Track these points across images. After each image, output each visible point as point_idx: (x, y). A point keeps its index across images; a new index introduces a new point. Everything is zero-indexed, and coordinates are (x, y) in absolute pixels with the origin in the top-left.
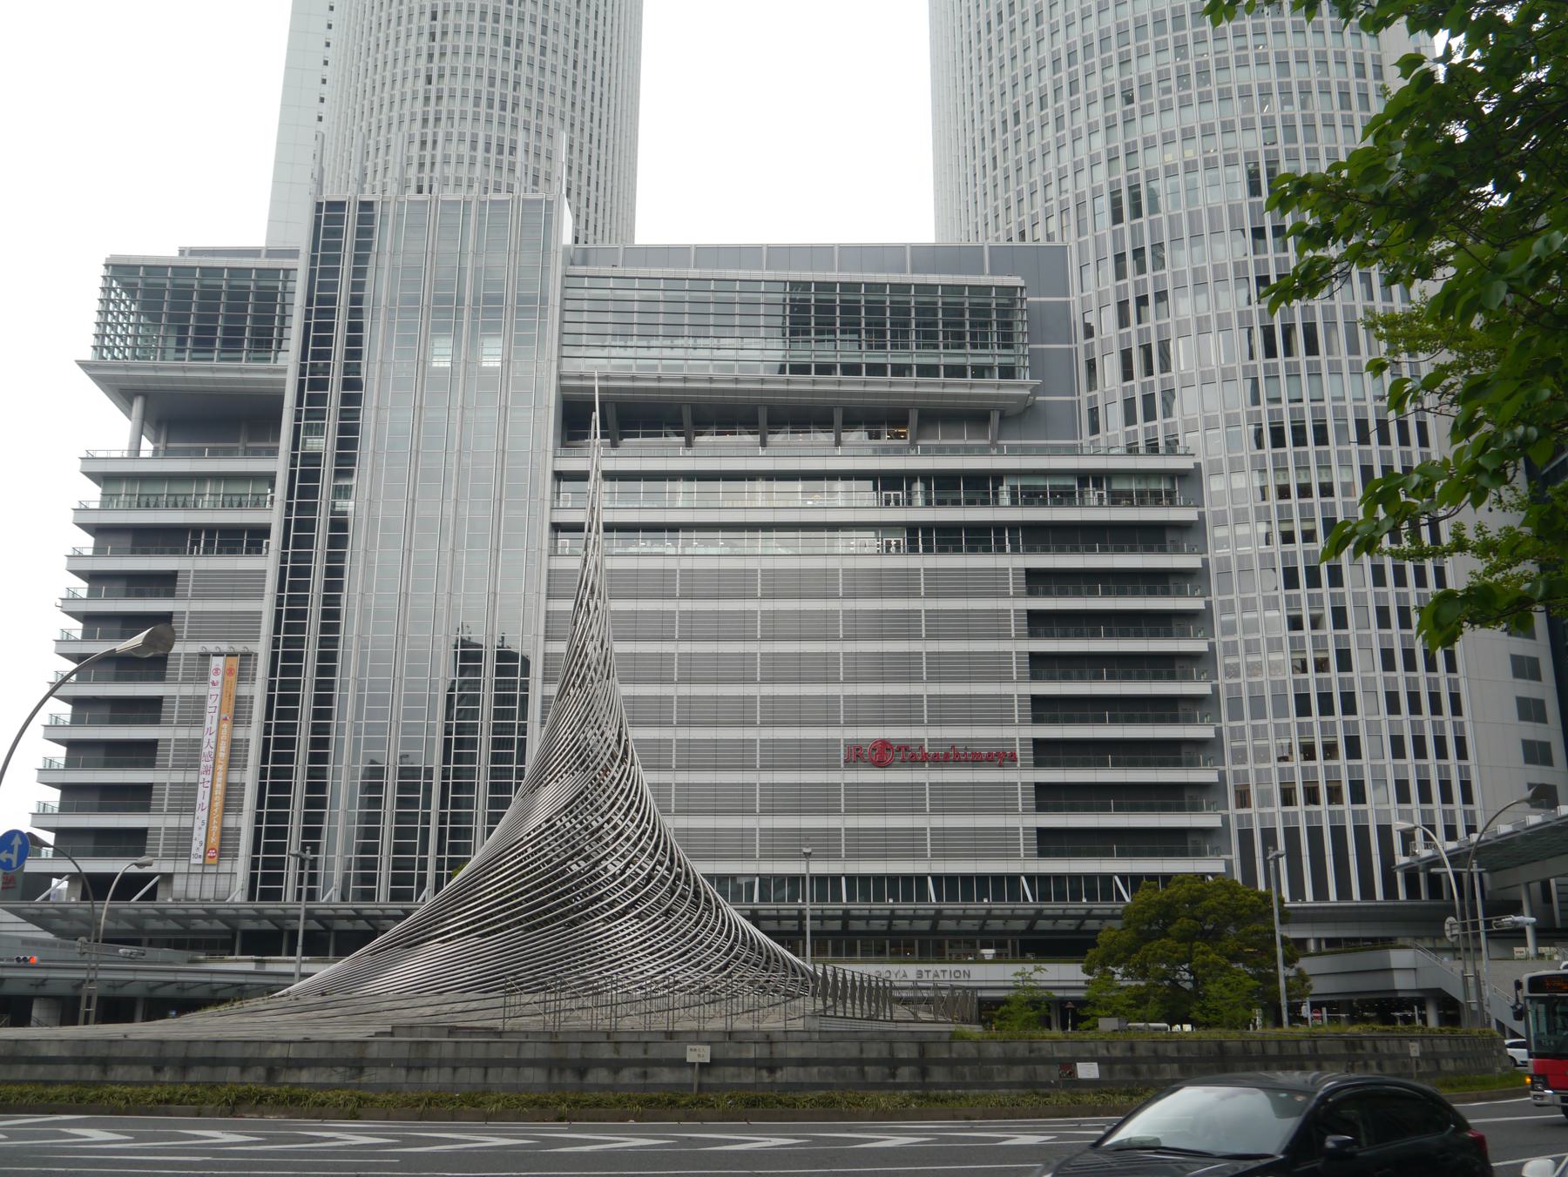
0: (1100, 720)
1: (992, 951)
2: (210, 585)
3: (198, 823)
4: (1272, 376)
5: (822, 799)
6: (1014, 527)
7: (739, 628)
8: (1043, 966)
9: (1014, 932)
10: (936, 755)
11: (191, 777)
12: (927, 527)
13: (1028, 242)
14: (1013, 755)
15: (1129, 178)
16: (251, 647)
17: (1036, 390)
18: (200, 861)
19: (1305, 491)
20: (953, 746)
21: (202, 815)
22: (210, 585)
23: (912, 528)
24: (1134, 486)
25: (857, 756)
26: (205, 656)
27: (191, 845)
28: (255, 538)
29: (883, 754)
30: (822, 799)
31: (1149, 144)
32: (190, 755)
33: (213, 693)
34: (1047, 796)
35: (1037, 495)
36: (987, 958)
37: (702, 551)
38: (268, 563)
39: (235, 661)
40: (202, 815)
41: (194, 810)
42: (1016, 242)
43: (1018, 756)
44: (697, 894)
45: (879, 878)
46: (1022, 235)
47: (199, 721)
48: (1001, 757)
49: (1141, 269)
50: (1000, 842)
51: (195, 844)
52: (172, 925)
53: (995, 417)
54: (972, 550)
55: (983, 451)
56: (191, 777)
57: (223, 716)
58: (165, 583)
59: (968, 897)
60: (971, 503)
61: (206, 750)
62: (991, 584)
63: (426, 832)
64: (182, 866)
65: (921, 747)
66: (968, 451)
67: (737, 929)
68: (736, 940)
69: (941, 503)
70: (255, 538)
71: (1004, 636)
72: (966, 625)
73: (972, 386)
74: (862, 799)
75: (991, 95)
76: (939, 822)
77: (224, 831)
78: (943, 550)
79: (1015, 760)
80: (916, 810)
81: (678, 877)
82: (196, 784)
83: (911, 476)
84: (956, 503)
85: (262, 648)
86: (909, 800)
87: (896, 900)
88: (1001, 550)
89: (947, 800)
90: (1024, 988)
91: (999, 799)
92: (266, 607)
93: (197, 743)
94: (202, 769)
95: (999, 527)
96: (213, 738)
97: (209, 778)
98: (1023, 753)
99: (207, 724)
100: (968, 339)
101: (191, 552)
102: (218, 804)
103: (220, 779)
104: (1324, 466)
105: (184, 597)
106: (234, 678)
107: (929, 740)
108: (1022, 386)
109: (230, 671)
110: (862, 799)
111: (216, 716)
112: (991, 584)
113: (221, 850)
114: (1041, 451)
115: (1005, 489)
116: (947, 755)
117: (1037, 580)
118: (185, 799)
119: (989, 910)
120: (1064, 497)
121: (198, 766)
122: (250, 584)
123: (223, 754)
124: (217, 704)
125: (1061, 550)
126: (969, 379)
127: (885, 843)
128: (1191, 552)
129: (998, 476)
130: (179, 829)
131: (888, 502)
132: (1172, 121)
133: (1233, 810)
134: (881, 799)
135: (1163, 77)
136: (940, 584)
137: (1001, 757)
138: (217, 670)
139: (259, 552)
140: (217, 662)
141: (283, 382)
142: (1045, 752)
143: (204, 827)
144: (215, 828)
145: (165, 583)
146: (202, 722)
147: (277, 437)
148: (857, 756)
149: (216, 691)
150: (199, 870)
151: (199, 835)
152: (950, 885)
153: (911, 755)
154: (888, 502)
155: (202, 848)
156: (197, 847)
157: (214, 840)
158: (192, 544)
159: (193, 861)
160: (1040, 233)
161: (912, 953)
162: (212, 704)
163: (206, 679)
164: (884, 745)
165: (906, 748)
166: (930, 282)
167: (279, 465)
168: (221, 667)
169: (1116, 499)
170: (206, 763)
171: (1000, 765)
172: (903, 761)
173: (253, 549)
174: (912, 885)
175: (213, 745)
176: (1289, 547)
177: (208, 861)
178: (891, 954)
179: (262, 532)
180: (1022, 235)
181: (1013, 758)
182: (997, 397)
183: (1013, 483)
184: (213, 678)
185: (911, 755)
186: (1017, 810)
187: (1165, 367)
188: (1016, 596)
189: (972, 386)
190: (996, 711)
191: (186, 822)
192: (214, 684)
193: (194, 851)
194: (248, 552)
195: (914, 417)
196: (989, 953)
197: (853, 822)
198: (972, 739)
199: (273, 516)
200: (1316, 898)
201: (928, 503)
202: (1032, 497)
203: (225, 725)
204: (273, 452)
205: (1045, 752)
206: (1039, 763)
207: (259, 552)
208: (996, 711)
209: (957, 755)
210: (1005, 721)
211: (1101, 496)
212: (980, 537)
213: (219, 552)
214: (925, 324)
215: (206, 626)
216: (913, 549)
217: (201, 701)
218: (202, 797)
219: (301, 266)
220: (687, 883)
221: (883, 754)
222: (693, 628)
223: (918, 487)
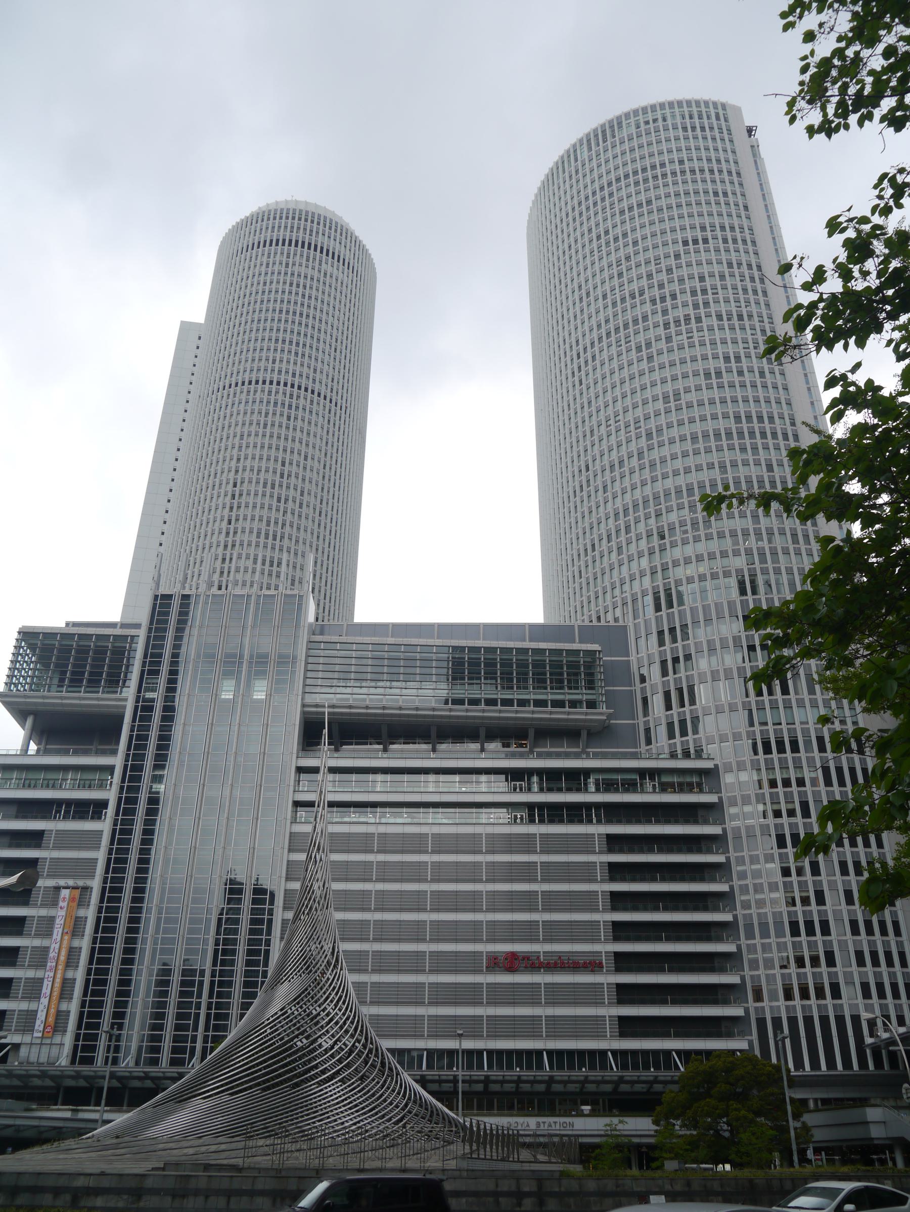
0: (658, 939)
1: (589, 1107)
2: (66, 840)
3: (41, 1007)
4: (761, 708)
5: (470, 994)
6: (598, 806)
7: (415, 873)
9: (604, 1093)
10: (549, 963)
11: (39, 974)
12: (541, 806)
13: (603, 623)
14: (601, 963)
15: (664, 584)
16: (89, 883)
17: (610, 716)
18: (40, 1035)
19: (787, 783)
20: (560, 957)
21: (44, 1001)
22: (66, 840)
23: (531, 806)
24: (675, 779)
25: (496, 963)
26: (58, 889)
27: (35, 1023)
28: (97, 809)
29: (512, 963)
30: (470, 994)
31: (676, 564)
32: (40, 957)
33: (60, 914)
34: (625, 994)
35: (613, 785)
36: (585, 1112)
37: (392, 820)
38: (105, 826)
39: (77, 893)
40: (44, 1001)
41: (39, 998)
42: (595, 623)
44: (383, 1064)
45: (509, 1052)
46: (599, 618)
47: (49, 934)
48: (592, 965)
49: (674, 640)
50: (592, 1027)
51: (38, 1022)
52: (16, 1082)
53: (584, 734)
54: (571, 821)
55: (577, 756)
56: (39, 974)
57: (66, 931)
58: (35, 838)
59: (571, 1067)
60: (569, 790)
61: (52, 954)
62: (583, 844)
63: (197, 1016)
64: (27, 1039)
65: (538, 957)
66: (567, 756)
67: (410, 1090)
68: (409, 1099)
69: (550, 790)
70: (97, 809)
71: (592, 880)
73: (569, 713)
74: (498, 995)
75: (577, 534)
76: (551, 1011)
77: (59, 1013)
78: (551, 821)
79: (602, 967)
80: (536, 1003)
81: (370, 1051)
82: (43, 979)
83: (530, 772)
84: (560, 790)
85: (96, 884)
86: (529, 994)
87: (522, 1068)
88: (590, 821)
89: (556, 995)
90: (611, 1136)
91: (590, 995)
92: (101, 855)
93: (46, 950)
94: (48, 968)
95: (588, 806)
96: (57, 946)
97: (52, 974)
99: (55, 936)
100: (566, 683)
101: (55, 817)
102: (56, 994)
103: (59, 976)
104: (798, 767)
105: (47, 848)
106: (75, 904)
107: (544, 952)
108: (601, 714)
109: (72, 899)
110: (498, 995)
111: (60, 930)
112: (583, 844)
113: (55, 1027)
114: (614, 756)
115: (591, 780)
116: (556, 963)
117: (614, 843)
118: (34, 989)
119: (587, 1077)
120: (630, 786)
121: (46, 966)
122: (91, 840)
123: (63, 958)
124: (62, 922)
125: (629, 822)
126: (567, 709)
127: (515, 1026)
128: (715, 823)
129: (587, 772)
130: (28, 1011)
131: (515, 789)
132: (689, 550)
133: (751, 1004)
134: (513, 995)
135: (682, 524)
136: (550, 844)
137: (592, 965)
138: (64, 898)
139: (100, 818)
140: (65, 893)
141: (125, 707)
142: (623, 962)
143: (45, 1011)
144: (53, 1011)
145: (35, 838)
146: (51, 935)
147: (118, 742)
148: (496, 963)
149: (62, 913)
150: (39, 1041)
151: (41, 1016)
152: (558, 1056)
153: (531, 963)
154: (515, 789)
155: (42, 1026)
156: (39, 1025)
157: (51, 1019)
158: (56, 813)
159: (36, 1035)
160: (610, 617)
161: (533, 1108)
162: (59, 922)
163: (57, 905)
164: (513, 955)
165: (528, 958)
166: (541, 647)
167: (117, 761)
168: (67, 897)
170: (51, 964)
171: (592, 971)
172: (526, 967)
173: (96, 816)
174: (531, 1058)
175: (57, 951)
176: (779, 821)
177: (46, 1035)
178: (518, 1109)
179: (104, 804)
180: (599, 618)
181: (600, 965)
182: (585, 720)
183: (597, 777)
184: (61, 904)
185: (531, 963)
186: (604, 1003)
187: (693, 702)
188: (601, 852)
189: (569, 713)
190: (588, 932)
191: (33, 1006)
192: (61, 908)
193: (36, 1027)
194: (92, 818)
195: (531, 733)
196: (587, 1108)
197: (492, 1011)
198: (573, 952)
199: (111, 795)
200: (812, 1068)
201: (541, 790)
202: (609, 786)
203: (66, 937)
204: (114, 752)
205: (623, 962)
206: (619, 969)
207: (100, 818)
208: (588, 932)
209: (563, 963)
210: (595, 940)
211: (654, 786)
212: (575, 813)
213: (74, 818)
214: (539, 674)
215: (60, 868)
216: (532, 821)
217: (52, 920)
218: (46, 989)
219: (142, 633)
220: (376, 1056)
221: (512, 963)
222: (386, 873)
223: (535, 779)
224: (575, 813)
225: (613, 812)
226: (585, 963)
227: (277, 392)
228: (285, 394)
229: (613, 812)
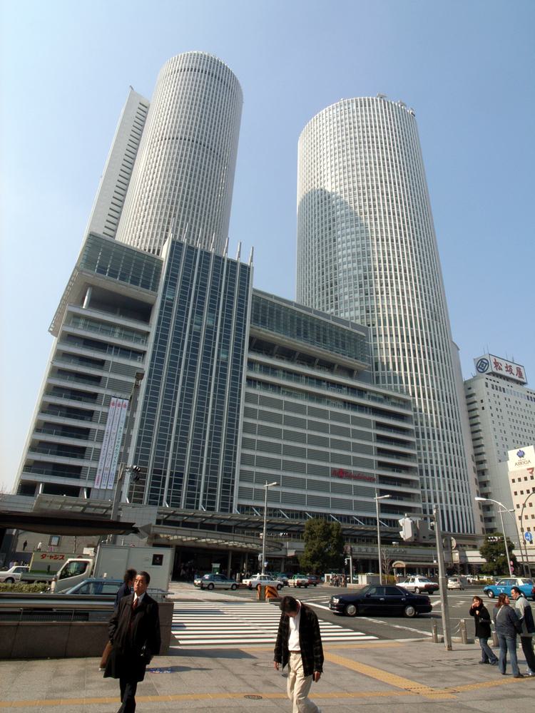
22: (118, 368)
28: (140, 354)
29: (340, 474)
62: (365, 423)
86: (346, 489)
112: (365, 423)
117: (379, 425)
120: (380, 401)
141: (155, 302)
145: (100, 364)
169: (394, 404)
179: (143, 353)
199: (149, 348)
202: (374, 399)
212: (362, 408)
221: (340, 474)
222: (289, 421)
224: (362, 408)
225: (376, 411)
229: (376, 411)
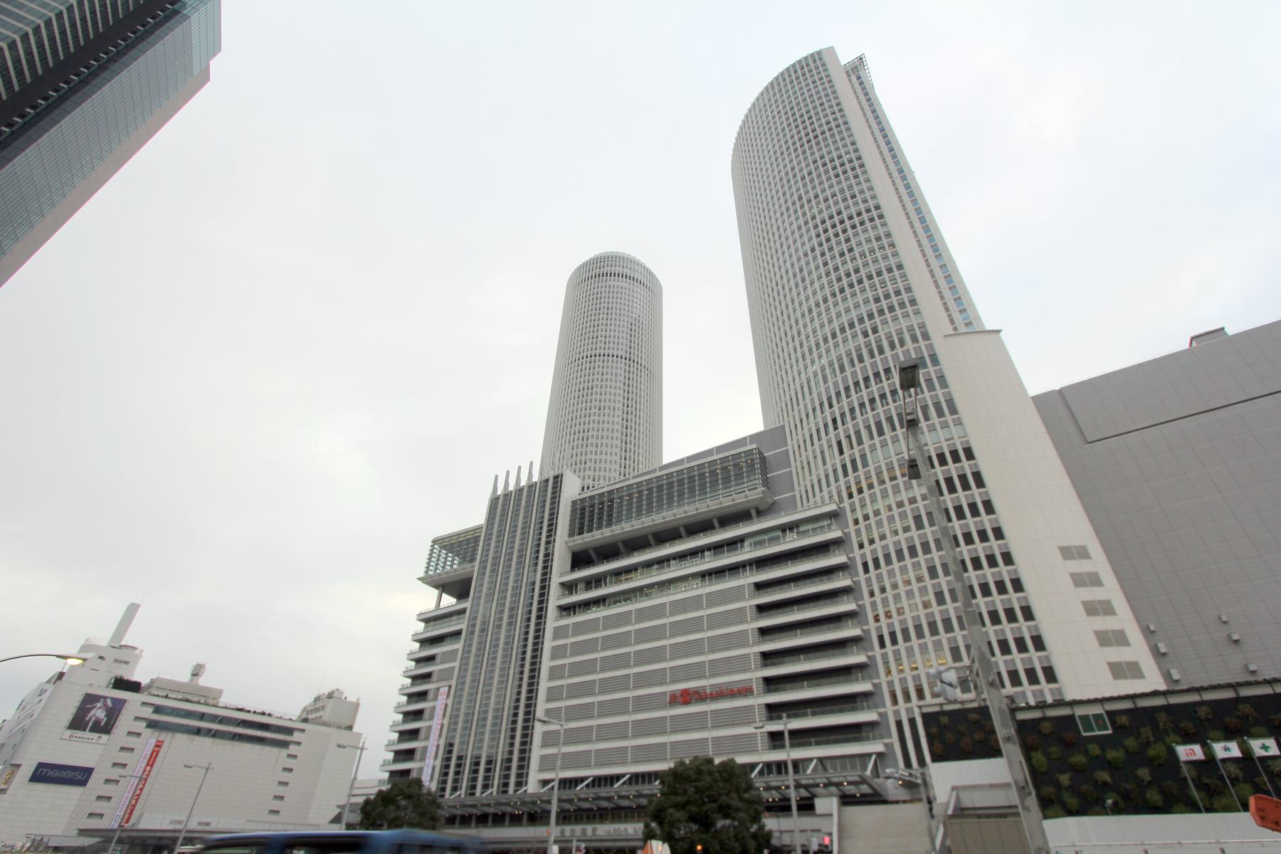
8: (171, 827)
29: (686, 697)
43: (755, 689)
62: (736, 594)
72: (725, 619)
80: (703, 728)
98: (757, 687)
112: (736, 594)
133: (889, 708)
136: (713, 599)
137: (746, 691)
140: (441, 690)
142: (772, 683)
164: (685, 692)
172: (696, 700)
205: (772, 683)
208: (740, 664)
221: (686, 697)
226: (738, 690)
227: (608, 361)
228: (613, 361)
